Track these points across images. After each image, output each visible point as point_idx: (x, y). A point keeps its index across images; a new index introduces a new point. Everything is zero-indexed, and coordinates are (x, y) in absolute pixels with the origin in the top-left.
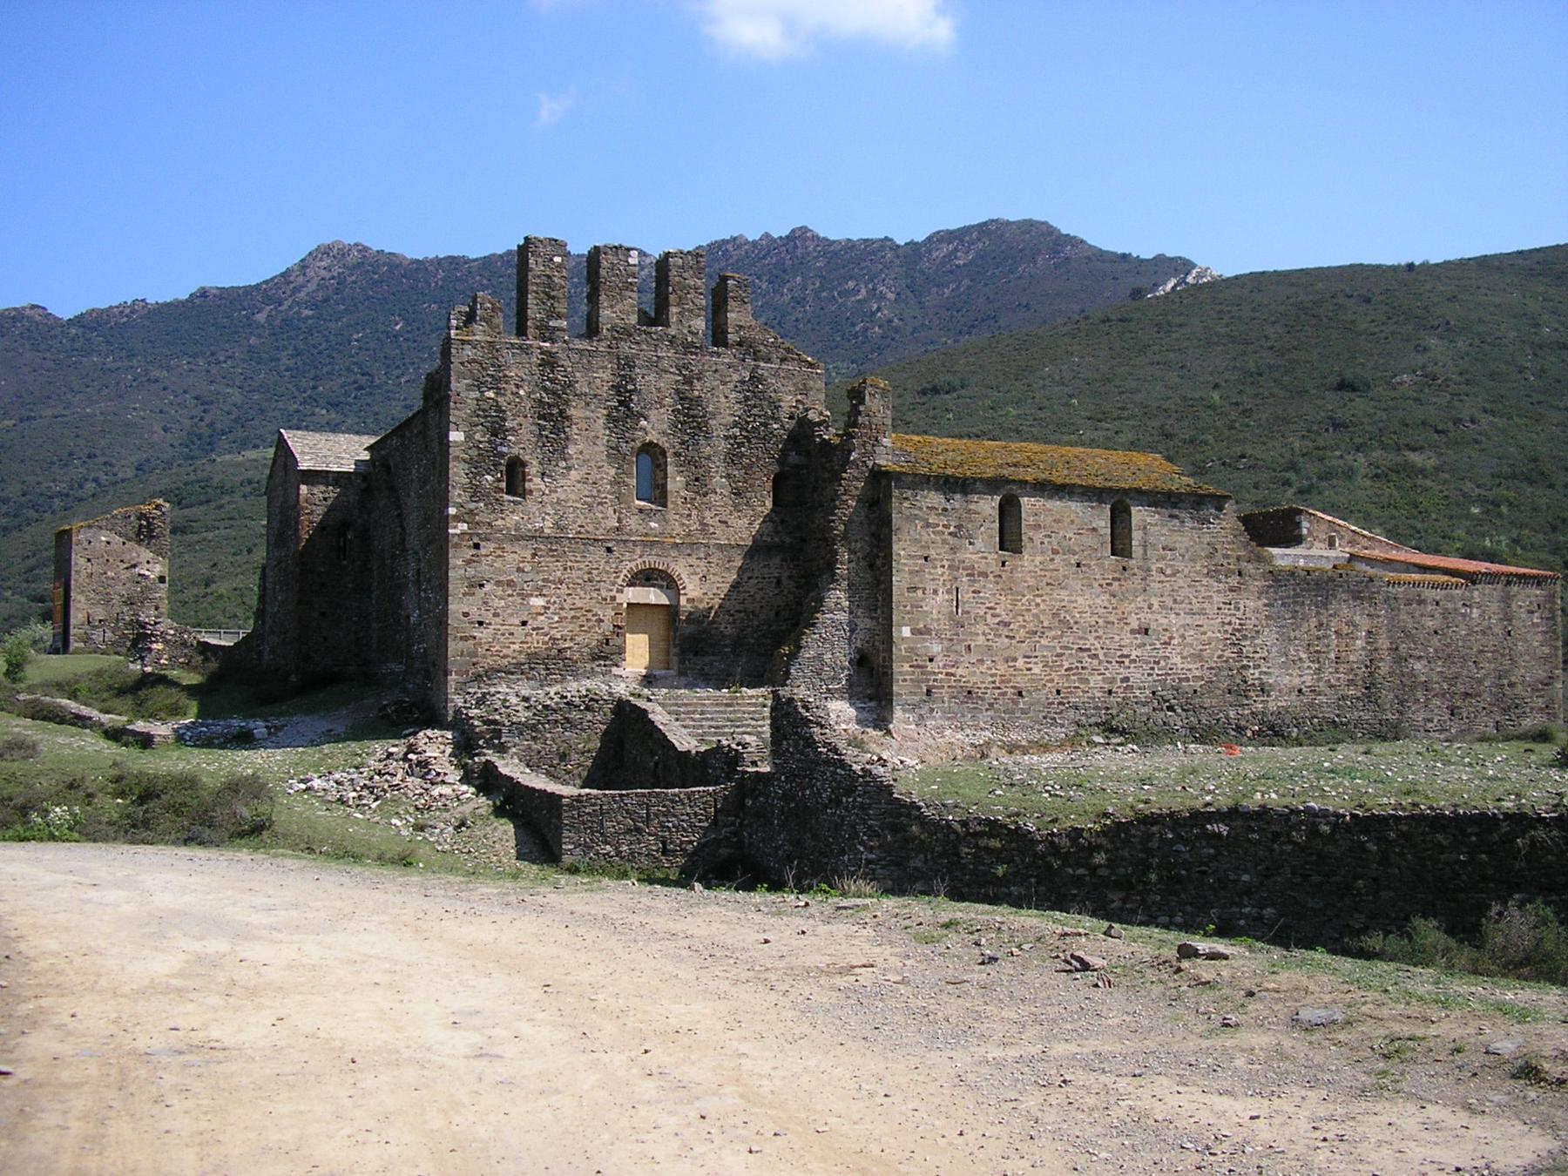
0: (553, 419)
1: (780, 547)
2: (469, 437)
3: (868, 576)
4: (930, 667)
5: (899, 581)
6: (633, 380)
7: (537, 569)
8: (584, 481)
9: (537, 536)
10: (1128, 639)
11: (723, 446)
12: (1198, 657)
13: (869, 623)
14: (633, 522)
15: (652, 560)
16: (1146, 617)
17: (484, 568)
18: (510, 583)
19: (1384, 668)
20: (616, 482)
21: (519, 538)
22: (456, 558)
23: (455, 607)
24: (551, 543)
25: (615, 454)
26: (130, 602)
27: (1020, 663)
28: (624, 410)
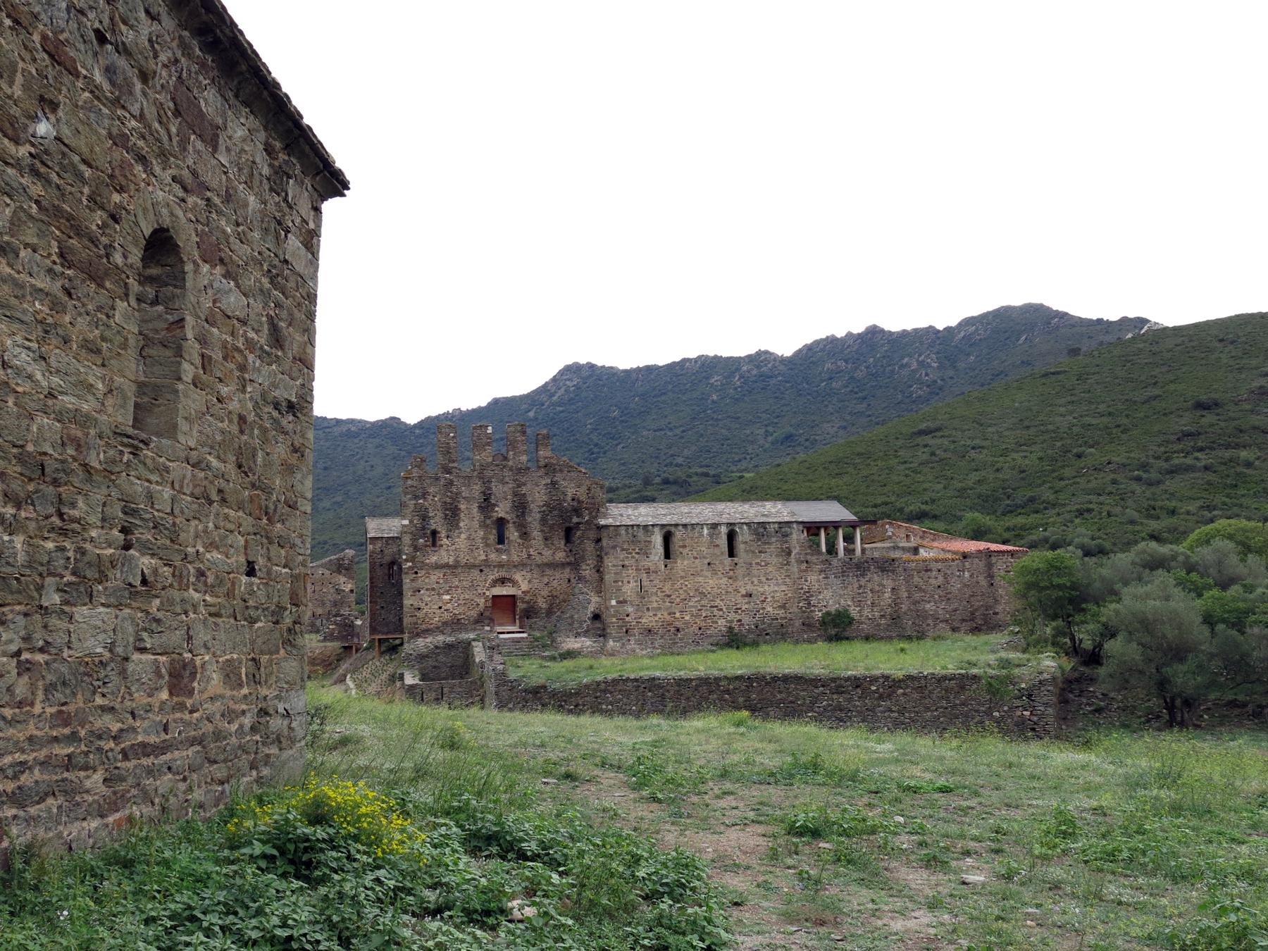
0: (452, 514)
1: (569, 564)
2: (411, 522)
3: (596, 575)
4: (627, 619)
5: (608, 578)
6: (490, 489)
7: (446, 581)
8: (468, 538)
9: (447, 566)
10: (740, 600)
11: (538, 516)
12: (783, 607)
13: (598, 599)
14: (493, 556)
15: (503, 574)
16: (749, 588)
17: (419, 583)
18: (433, 589)
19: (904, 607)
20: (485, 538)
21: (438, 567)
22: (406, 580)
23: (407, 602)
24: (453, 568)
25: (483, 525)
26: (335, 604)
27: (678, 615)
28: (487, 504)
